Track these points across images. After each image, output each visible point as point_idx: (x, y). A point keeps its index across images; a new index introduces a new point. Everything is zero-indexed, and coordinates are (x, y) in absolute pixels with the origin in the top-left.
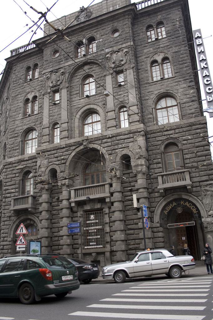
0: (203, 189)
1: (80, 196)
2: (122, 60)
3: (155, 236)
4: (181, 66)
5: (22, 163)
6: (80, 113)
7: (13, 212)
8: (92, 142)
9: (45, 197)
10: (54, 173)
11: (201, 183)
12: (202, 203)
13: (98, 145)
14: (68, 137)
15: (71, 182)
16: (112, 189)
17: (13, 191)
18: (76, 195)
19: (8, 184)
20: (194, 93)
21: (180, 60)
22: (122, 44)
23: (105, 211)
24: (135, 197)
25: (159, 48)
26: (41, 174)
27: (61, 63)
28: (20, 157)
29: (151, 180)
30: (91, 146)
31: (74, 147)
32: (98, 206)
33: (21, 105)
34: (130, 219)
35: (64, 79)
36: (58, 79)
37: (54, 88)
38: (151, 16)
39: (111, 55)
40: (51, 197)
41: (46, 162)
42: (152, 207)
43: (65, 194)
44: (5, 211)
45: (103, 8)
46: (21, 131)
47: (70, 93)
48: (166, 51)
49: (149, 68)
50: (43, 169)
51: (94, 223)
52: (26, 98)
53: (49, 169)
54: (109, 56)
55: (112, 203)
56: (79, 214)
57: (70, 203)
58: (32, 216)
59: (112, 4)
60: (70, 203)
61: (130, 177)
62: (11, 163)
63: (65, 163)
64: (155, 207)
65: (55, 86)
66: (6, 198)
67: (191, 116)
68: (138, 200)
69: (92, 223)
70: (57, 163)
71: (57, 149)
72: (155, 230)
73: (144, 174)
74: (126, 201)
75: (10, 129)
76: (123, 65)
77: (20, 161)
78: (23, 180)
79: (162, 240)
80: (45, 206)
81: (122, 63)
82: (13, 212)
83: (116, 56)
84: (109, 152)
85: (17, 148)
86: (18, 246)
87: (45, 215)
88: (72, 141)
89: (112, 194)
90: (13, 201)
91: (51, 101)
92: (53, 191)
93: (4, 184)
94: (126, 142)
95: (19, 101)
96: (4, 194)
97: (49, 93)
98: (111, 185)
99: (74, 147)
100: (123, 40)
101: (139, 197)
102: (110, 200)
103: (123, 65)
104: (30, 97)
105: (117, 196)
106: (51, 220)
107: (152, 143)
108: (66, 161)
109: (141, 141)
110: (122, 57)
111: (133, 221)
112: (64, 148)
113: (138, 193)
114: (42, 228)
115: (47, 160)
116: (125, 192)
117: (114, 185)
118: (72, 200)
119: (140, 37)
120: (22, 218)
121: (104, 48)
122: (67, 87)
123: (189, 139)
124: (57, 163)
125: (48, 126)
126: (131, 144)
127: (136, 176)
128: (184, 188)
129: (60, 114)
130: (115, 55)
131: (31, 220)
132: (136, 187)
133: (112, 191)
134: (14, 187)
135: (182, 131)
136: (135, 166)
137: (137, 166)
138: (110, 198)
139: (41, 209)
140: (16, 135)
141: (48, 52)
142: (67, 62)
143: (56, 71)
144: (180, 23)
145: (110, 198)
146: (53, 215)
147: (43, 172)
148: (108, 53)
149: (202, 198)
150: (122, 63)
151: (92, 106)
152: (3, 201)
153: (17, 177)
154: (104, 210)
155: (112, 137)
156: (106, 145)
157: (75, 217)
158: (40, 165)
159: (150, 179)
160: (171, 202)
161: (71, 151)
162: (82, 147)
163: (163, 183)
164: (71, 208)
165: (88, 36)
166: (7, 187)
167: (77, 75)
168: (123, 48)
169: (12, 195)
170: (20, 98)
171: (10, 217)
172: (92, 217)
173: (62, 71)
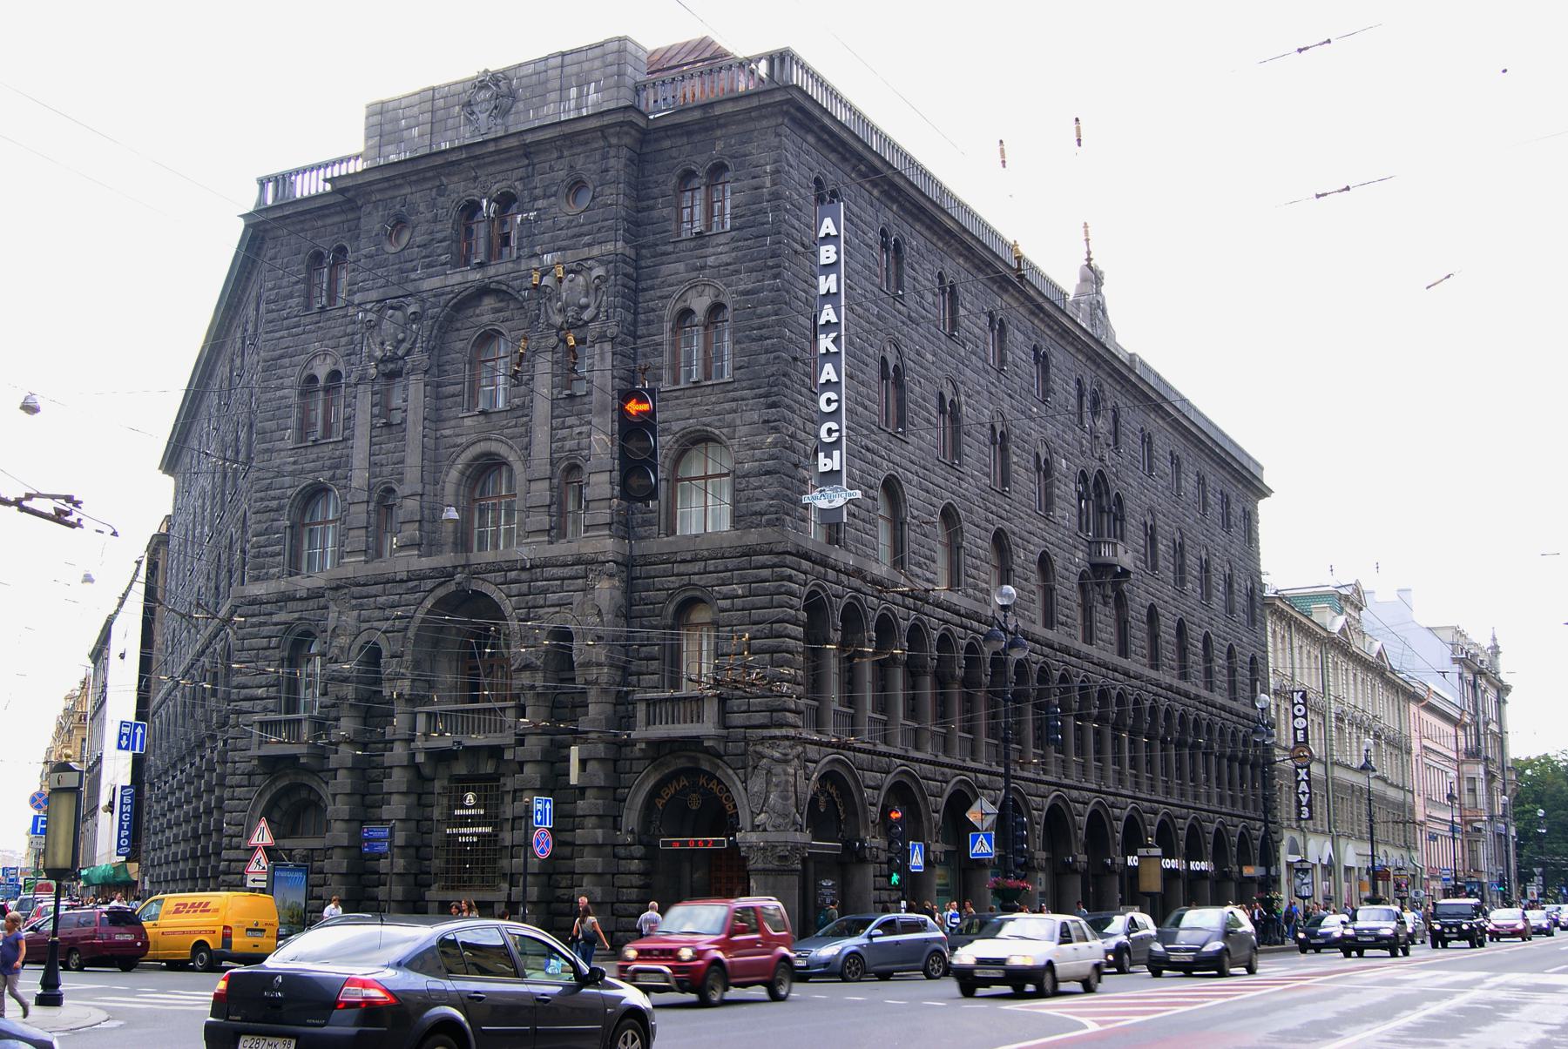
2: (585, 307)
4: (754, 346)
7: (255, 762)
10: (373, 656)
14: (420, 545)
20: (774, 444)
21: (757, 322)
22: (590, 245)
24: (574, 752)
25: (703, 268)
27: (413, 276)
28: (283, 585)
30: (477, 585)
31: (429, 584)
32: (489, 768)
33: (293, 396)
36: (401, 336)
37: (391, 366)
38: (697, 138)
41: (350, 618)
43: (399, 721)
44: (237, 756)
45: (549, 86)
46: (289, 492)
47: (436, 392)
48: (719, 284)
49: (667, 336)
50: (343, 641)
51: (472, 816)
53: (363, 638)
56: (438, 786)
59: (577, 75)
62: (254, 601)
65: (392, 359)
66: (239, 712)
67: (756, 519)
68: (583, 763)
69: (467, 817)
70: (385, 625)
72: (622, 851)
74: (554, 760)
75: (258, 479)
76: (586, 323)
77: (285, 599)
79: (636, 880)
81: (586, 316)
82: (255, 762)
83: (571, 289)
85: (277, 548)
86: (250, 877)
87: (343, 780)
91: (376, 410)
92: (373, 710)
95: (287, 382)
99: (429, 584)
100: (596, 227)
104: (322, 371)
105: (534, 745)
106: (364, 796)
107: (644, 594)
109: (606, 590)
112: (402, 581)
115: (355, 613)
118: (419, 744)
119: (655, 214)
120: (284, 782)
121: (538, 249)
122: (426, 372)
123: (738, 597)
124: (385, 625)
126: (578, 596)
128: (694, 742)
129: (402, 462)
131: (311, 789)
135: (721, 568)
136: (581, 665)
137: (587, 665)
139: (333, 761)
140: (274, 504)
141: (373, 222)
144: (774, 184)
147: (342, 649)
150: (586, 316)
151: (494, 447)
152: (231, 722)
156: (515, 588)
160: (675, 775)
162: (452, 587)
163: (648, 724)
165: (496, 189)
167: (459, 325)
169: (259, 705)
170: (289, 371)
171: (250, 774)
172: (470, 798)
173: (411, 309)
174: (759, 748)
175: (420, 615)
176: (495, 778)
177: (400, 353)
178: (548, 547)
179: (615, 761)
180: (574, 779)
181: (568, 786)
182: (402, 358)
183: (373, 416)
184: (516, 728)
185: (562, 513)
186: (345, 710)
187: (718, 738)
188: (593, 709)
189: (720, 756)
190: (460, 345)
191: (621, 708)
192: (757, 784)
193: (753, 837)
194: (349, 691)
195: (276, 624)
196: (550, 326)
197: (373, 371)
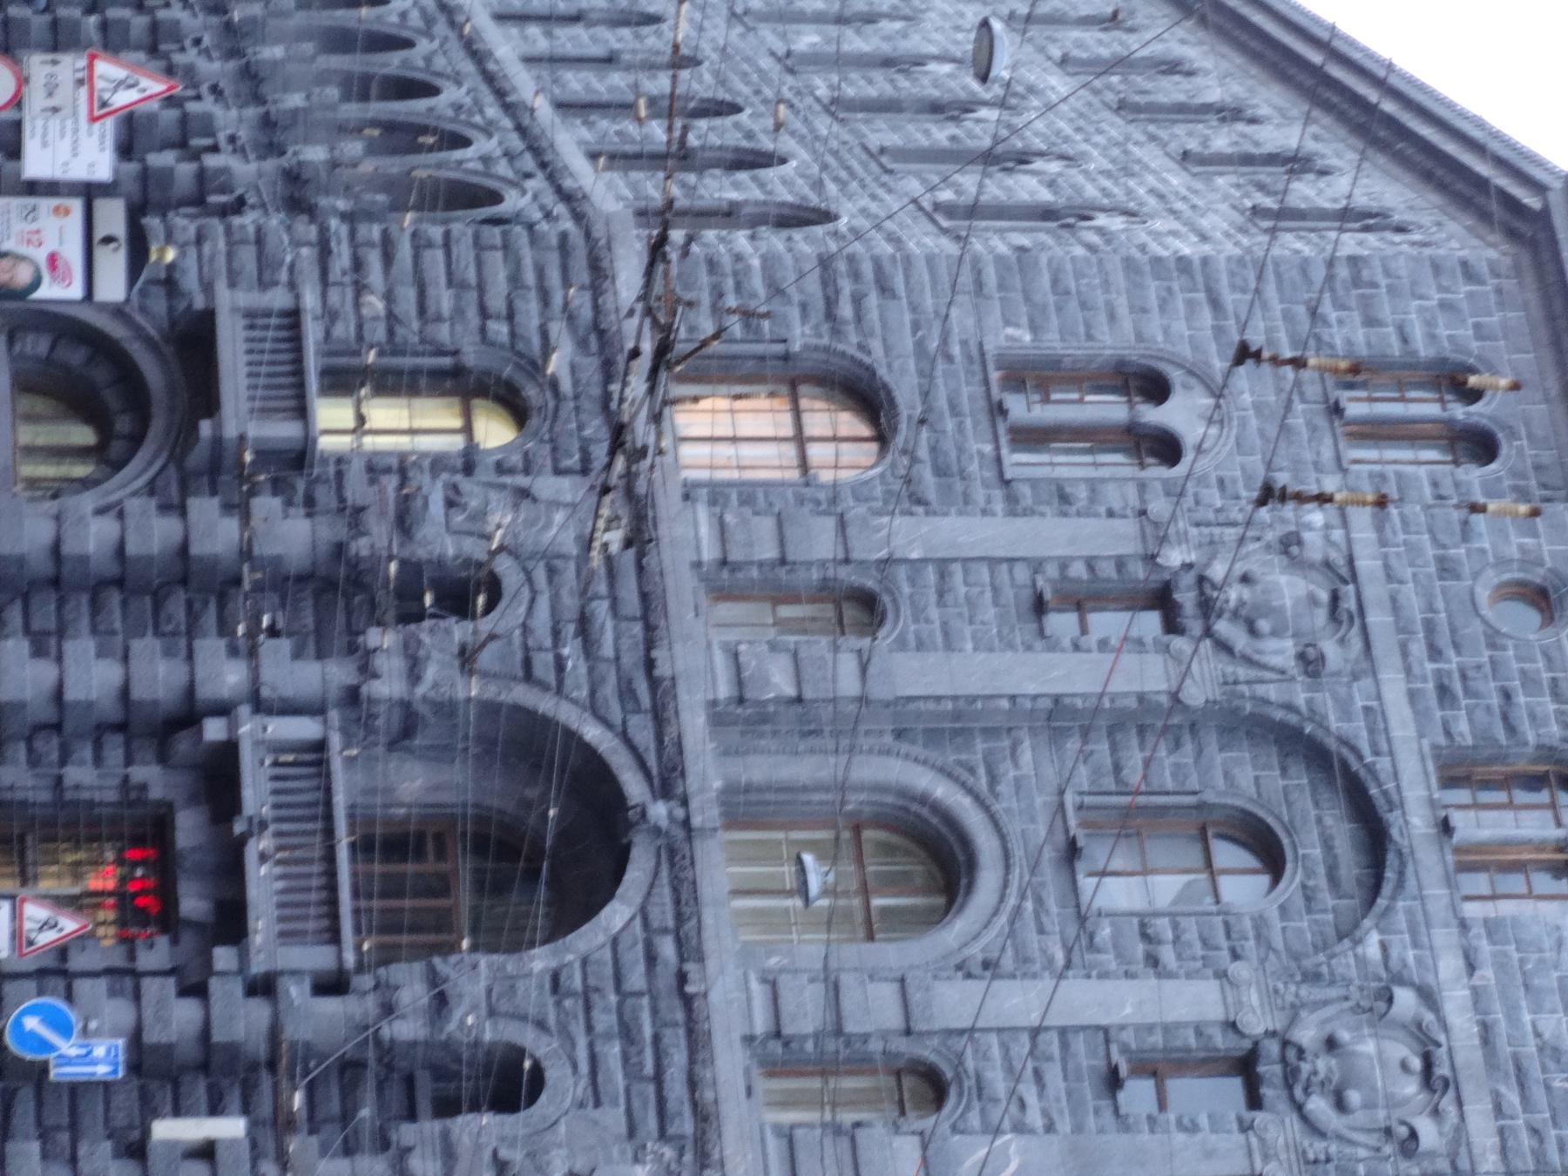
2: (1340, 1105)
5: (591, 367)
6: (942, 791)
7: (199, 303)
8: (672, 865)
9: (290, 534)
13: (638, 900)
14: (741, 700)
15: (386, 722)
16: (296, 992)
17: (374, 304)
19: (435, 260)
23: (152, 946)
24: (230, 1128)
26: (464, 507)
27: (1418, 648)
31: (644, 735)
32: (193, 903)
33: (1114, 341)
34: (82, 1107)
35: (1253, 673)
39: (1404, 1027)
40: (286, 584)
41: (560, 532)
46: (876, 345)
52: (1176, 376)
53: (505, 567)
54: (1395, 1009)
55: (196, 989)
58: (155, 457)
60: (223, 709)
63: (528, 676)
65: (1207, 608)
66: (324, 251)
68: (206, 1151)
71: (645, 618)
76: (1299, 1108)
78: (458, 372)
80: (214, 531)
81: (1318, 1105)
84: (571, 977)
87: (154, 534)
88: (693, 724)
89: (263, 987)
90: (278, 299)
92: (335, 597)
93: (436, 232)
94: (634, 1093)
96: (353, 234)
97: (1150, 559)
101: (221, 1155)
102: (223, 974)
103: (1299, 1108)
104: (1180, 413)
105: (241, 1021)
108: (544, 686)
110: (1369, 1105)
111: (65, 1121)
112: (650, 664)
113: (246, 1154)
114: (58, 518)
118: (248, 726)
125: (855, 555)
126: (613, 1118)
130: (1401, 1050)
131: (136, 440)
134: (407, 297)
136: (446, 1135)
139: (204, 508)
140: (846, 310)
142: (1413, 696)
143: (1349, 603)
146: (155, 594)
147: (481, 515)
148: (1428, 996)
150: (1318, 1105)
153: (483, 330)
154: (162, 942)
155: (688, 1001)
158: (535, 500)
161: (616, 714)
162: (634, 787)
164: (189, 714)
166: (404, 251)
168: (1462, 1117)
173: (1330, 648)
175: (568, 714)
176: (168, 921)
177: (1222, 627)
178: (736, 1036)
180: (166, 1130)
181: (149, 1111)
182: (1208, 632)
183: (1064, 564)
184: (291, 969)
185: (825, 1067)
186: (328, 530)
190: (1246, 778)
194: (377, 538)
195: (544, 334)
196: (1295, 1012)
197: (1174, 557)
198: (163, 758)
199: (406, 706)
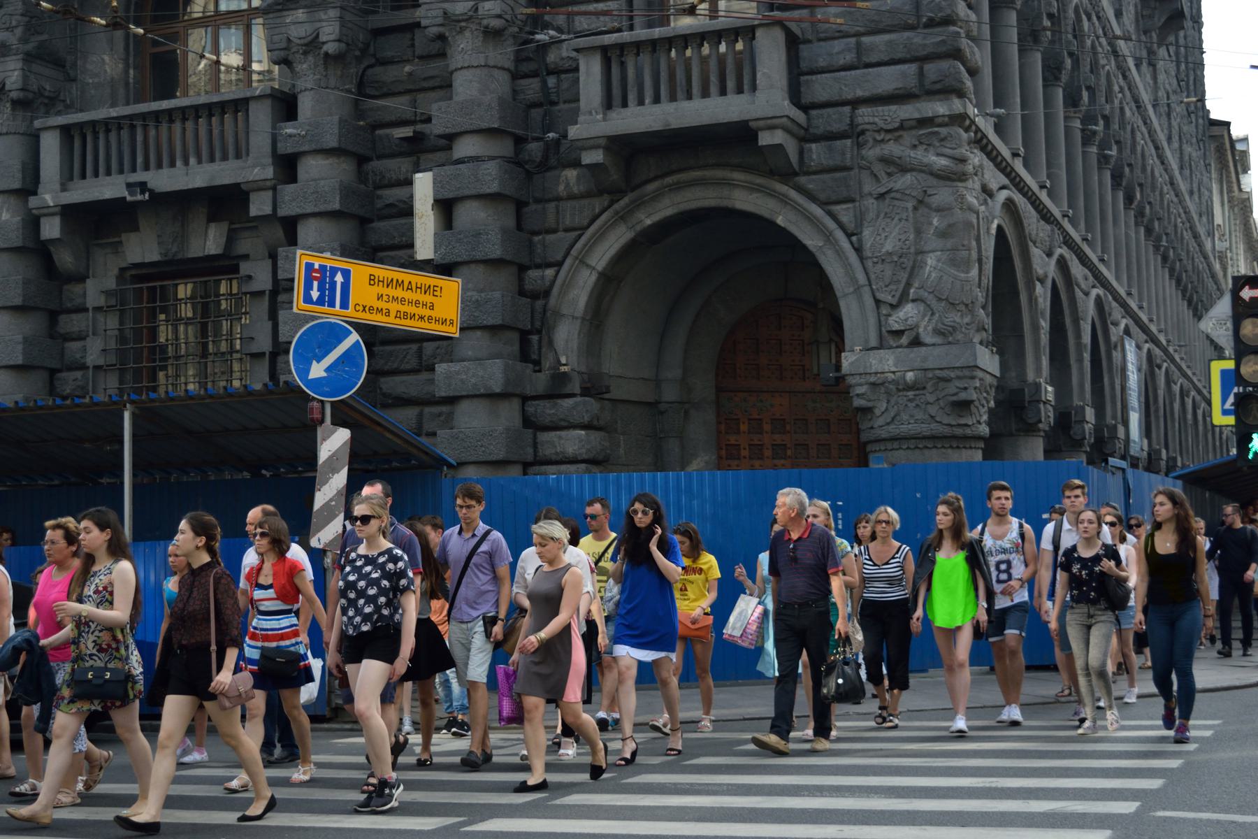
0: (872, 153)
1: (96, 175)
3: (547, 452)
11: (866, 115)
12: (858, 250)
18: (72, 172)
23: (250, 277)
24: (424, 186)
29: (544, 83)
32: (211, 241)
42: (538, 261)
55: (290, 229)
56: (94, 292)
57: (33, 222)
60: (33, 222)
61: (418, 52)
64: (559, 264)
68: (445, 207)
73: (492, 34)
89: (287, 166)
98: (286, 105)
111: (414, 347)
113: (449, 169)
116: (379, 157)
117: (306, 105)
118: (49, 196)
127: (440, 48)
128: (736, 141)
132: (437, 127)
133: (286, 148)
138: (274, 189)
145: (274, 189)
149: (860, 220)
154: (245, 268)
157: (70, 311)
159: (534, 74)
163: (608, 105)
174: (893, 149)
179: (520, 205)
187: (792, 129)
188: (466, 86)
189: (787, 174)
191: (531, 88)
192: (887, 237)
193: (886, 362)
198: (82, 279)
199: (29, 58)
